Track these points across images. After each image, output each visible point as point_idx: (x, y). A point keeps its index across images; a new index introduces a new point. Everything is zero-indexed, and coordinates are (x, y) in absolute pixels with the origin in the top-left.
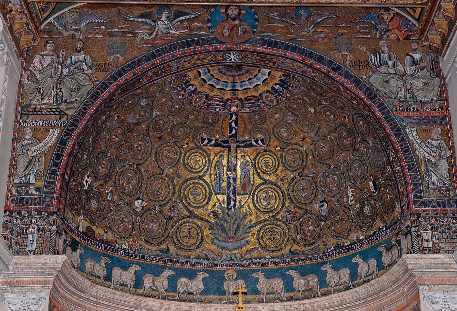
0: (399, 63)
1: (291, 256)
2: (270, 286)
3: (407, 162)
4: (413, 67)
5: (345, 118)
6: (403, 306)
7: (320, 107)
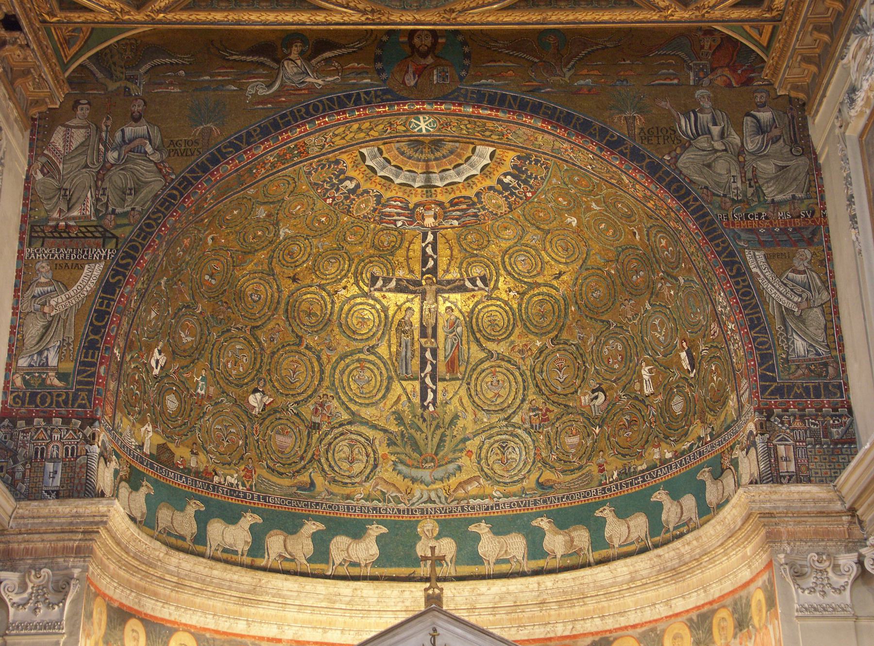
1: (540, 491)
2: (502, 547)
3: (748, 315)
5: (634, 234)
6: (744, 581)
7: (588, 215)
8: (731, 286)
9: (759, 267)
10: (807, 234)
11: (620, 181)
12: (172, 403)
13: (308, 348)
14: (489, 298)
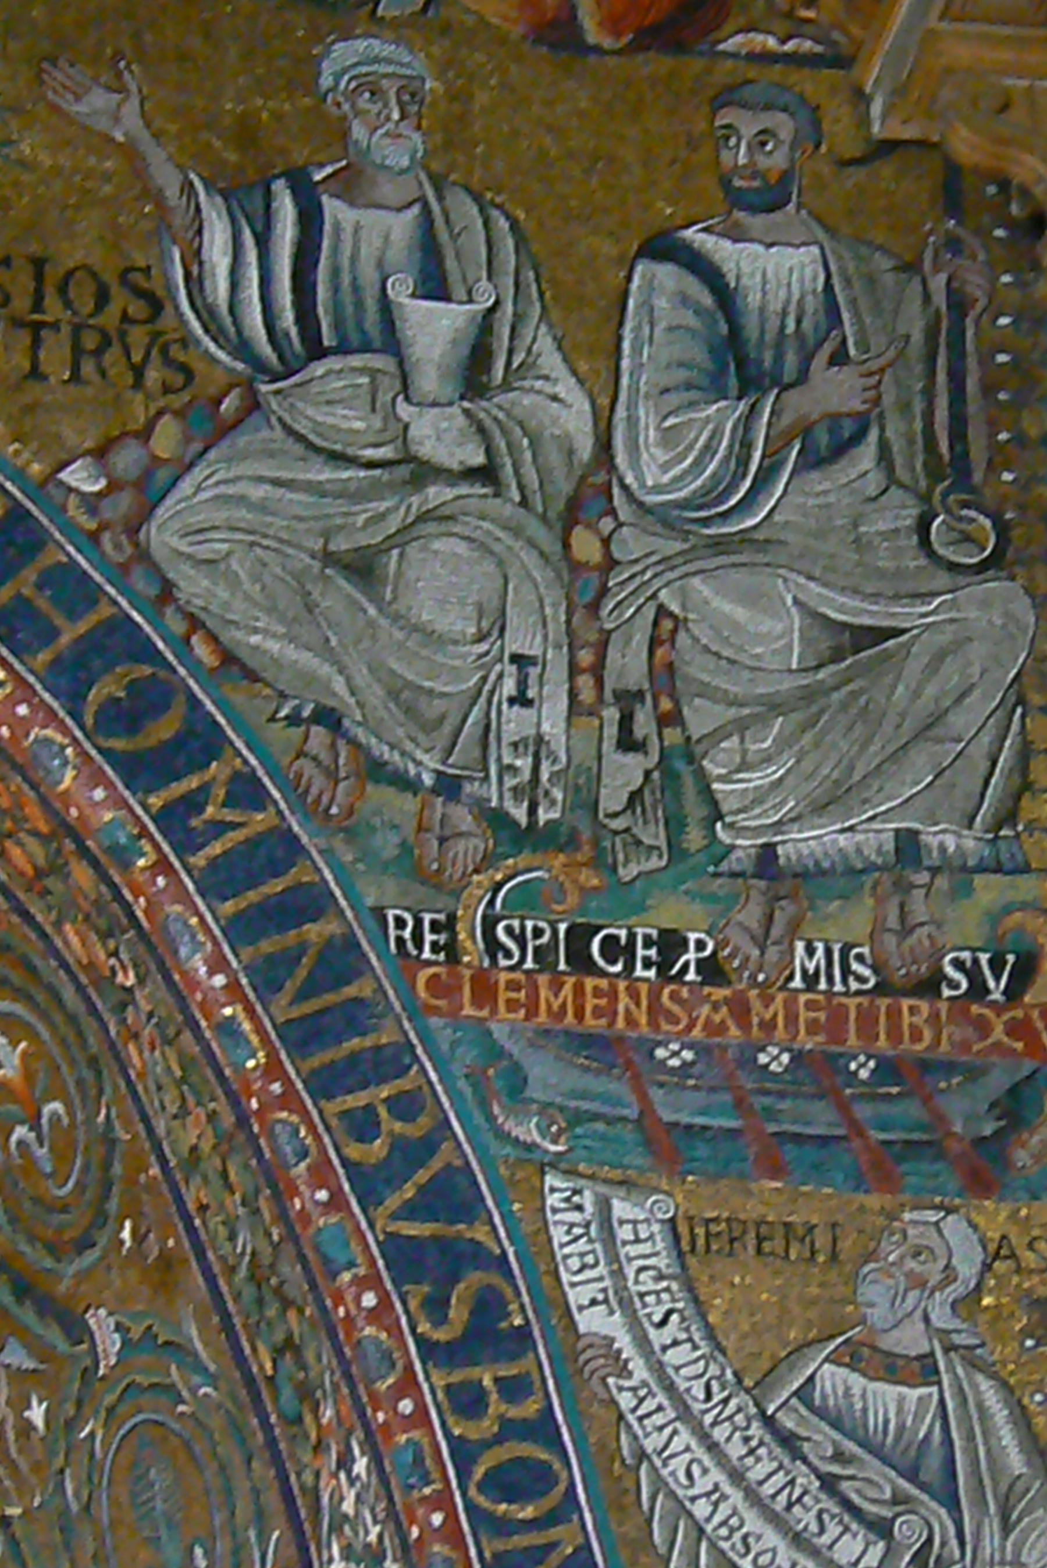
0: (545, 343)
8: (421, 1413)
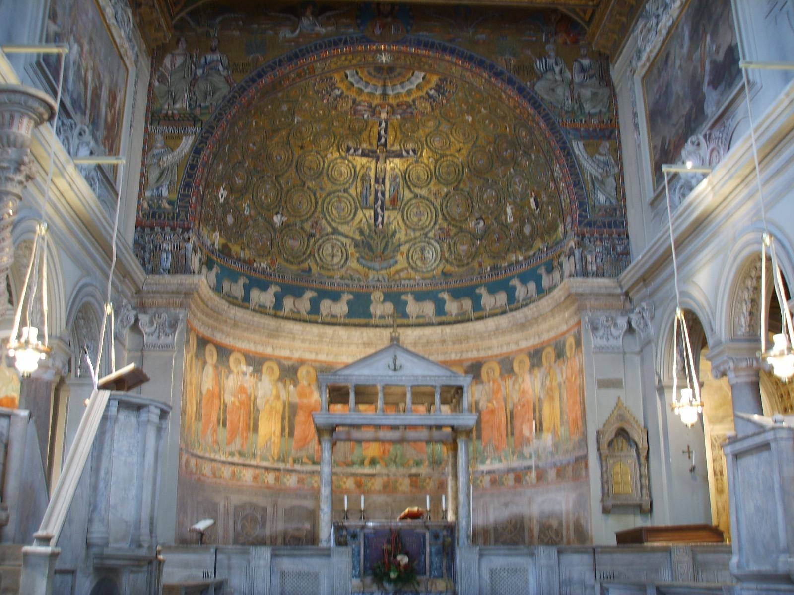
4: (582, 75)
9: (579, 150)
10: (607, 134)
11: (500, 97)
12: (230, 220)
13: (308, 188)
14: (417, 162)
